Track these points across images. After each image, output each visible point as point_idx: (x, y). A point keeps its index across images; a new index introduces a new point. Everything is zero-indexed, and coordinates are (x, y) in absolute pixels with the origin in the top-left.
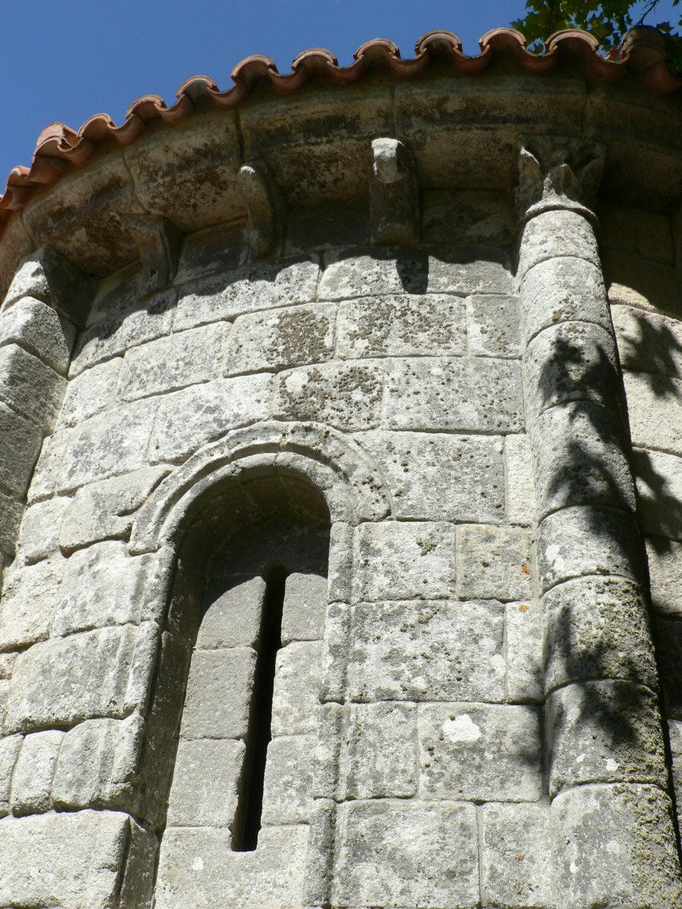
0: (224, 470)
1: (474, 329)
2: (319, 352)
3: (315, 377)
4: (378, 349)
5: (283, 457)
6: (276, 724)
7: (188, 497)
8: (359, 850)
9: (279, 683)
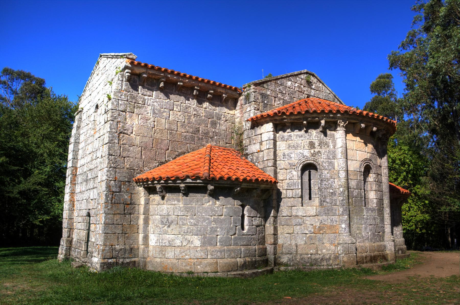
0: (305, 163)
1: (331, 145)
2: (314, 148)
3: (314, 151)
4: (321, 148)
5: (312, 162)
6: (312, 188)
7: (301, 165)
8: (324, 201)
9: (312, 184)
